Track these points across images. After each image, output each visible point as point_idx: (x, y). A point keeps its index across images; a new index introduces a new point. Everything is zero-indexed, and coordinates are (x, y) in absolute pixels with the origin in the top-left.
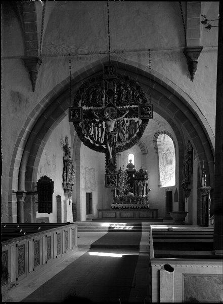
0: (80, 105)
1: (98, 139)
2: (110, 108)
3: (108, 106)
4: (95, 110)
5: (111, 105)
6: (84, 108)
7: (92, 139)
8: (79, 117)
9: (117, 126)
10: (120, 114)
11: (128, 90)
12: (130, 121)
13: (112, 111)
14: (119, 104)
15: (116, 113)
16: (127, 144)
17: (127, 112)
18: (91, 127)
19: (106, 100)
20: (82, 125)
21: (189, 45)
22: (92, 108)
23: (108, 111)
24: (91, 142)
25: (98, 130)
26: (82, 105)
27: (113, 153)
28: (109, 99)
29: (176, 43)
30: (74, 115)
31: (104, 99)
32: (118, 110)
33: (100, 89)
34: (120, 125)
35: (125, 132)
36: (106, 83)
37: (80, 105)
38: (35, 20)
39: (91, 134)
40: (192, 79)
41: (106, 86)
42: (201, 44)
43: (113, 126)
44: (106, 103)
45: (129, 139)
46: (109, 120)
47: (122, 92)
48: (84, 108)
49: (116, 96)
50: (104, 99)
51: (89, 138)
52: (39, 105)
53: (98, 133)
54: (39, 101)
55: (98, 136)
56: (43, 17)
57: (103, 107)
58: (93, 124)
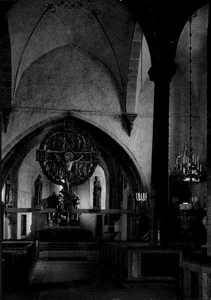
0: (45, 149)
1: (59, 175)
2: (69, 153)
3: (67, 151)
4: (56, 153)
5: (69, 151)
6: (49, 151)
9: (74, 167)
10: (75, 158)
12: (84, 163)
13: (70, 154)
17: (82, 156)
20: (47, 164)
21: (128, 111)
23: (67, 155)
26: (47, 149)
27: (70, 186)
29: (118, 110)
30: (40, 155)
31: (64, 146)
36: (66, 134)
37: (45, 149)
38: (11, 79)
40: (129, 135)
42: (136, 112)
43: (71, 166)
44: (66, 149)
46: (68, 162)
48: (49, 151)
50: (64, 146)
54: (10, 141)
56: (16, 76)
57: (63, 151)
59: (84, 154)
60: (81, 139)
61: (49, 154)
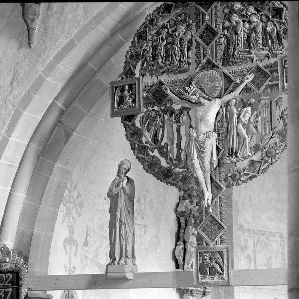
3: (203, 69)
7: (164, 154)
8: (134, 101)
11: (250, 22)
14: (227, 59)
15: (220, 83)
16: (252, 163)
18: (163, 126)
19: (198, 55)
20: (141, 121)
22: (164, 78)
24: (164, 163)
25: (179, 130)
28: (204, 49)
32: (225, 76)
33: (182, 28)
34: (232, 114)
35: (244, 131)
39: (163, 144)
41: (197, 21)
47: (234, 29)
49: (222, 40)
51: (156, 153)
52: (40, 76)
53: (180, 137)
55: (179, 145)
58: (166, 117)
59: (258, 69)
60: (246, 19)
61: (147, 89)
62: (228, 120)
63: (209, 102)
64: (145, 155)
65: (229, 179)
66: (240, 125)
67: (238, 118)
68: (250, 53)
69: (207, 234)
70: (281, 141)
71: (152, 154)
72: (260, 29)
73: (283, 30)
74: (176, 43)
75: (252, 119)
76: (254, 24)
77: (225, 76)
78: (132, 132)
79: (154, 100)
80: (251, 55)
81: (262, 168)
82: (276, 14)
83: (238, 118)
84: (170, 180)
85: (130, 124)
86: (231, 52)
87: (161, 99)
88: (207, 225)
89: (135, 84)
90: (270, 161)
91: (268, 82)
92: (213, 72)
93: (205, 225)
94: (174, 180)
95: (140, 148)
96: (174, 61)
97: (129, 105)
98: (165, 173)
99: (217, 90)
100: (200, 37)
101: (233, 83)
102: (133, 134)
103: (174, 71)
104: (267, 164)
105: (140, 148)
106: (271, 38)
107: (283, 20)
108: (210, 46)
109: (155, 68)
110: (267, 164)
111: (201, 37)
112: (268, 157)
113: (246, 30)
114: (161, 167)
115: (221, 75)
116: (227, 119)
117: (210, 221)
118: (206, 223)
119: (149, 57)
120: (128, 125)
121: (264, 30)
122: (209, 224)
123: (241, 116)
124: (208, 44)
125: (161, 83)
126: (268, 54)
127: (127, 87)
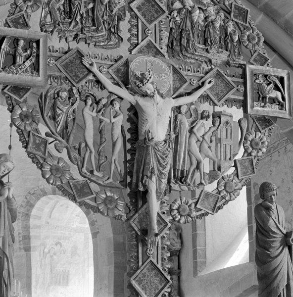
45: (212, 176)
48: (56, 43)
62: (177, 130)
63: (162, 100)
64: (47, 154)
65: (175, 212)
66: (193, 140)
67: (191, 131)
68: (208, 52)
69: (144, 289)
70: (244, 174)
71: (54, 152)
72: (218, 25)
73: (248, 36)
74: (105, 4)
75: (206, 137)
76: (213, 18)
77: (175, 71)
78: (24, 114)
79: (64, 74)
80: (209, 56)
81: (218, 205)
82: (240, 15)
83: (191, 131)
84: (87, 200)
85: (21, 100)
86: (184, 42)
87: (77, 76)
88: (144, 275)
89: (38, 42)
90: (227, 198)
91: (230, 95)
92: (157, 60)
93: (141, 275)
94: (95, 200)
95: (37, 142)
96: (102, 29)
97: (26, 70)
98: (79, 188)
99: (164, 87)
100: (137, 8)
101: (187, 84)
102: (27, 117)
103: (99, 42)
104: (224, 200)
105: (37, 142)
106: (232, 40)
107: (248, 25)
108: (153, 25)
109: (71, 28)
110: (224, 200)
111: (139, 8)
112: (227, 191)
113: (200, 21)
114: (72, 178)
115: (169, 67)
116: (175, 129)
117: (148, 269)
118: (143, 272)
119: (59, 9)
120: (18, 103)
121: (224, 29)
122: (147, 273)
123: (195, 130)
124: (150, 22)
125: (80, 55)
126: (228, 61)
127: (22, 43)
